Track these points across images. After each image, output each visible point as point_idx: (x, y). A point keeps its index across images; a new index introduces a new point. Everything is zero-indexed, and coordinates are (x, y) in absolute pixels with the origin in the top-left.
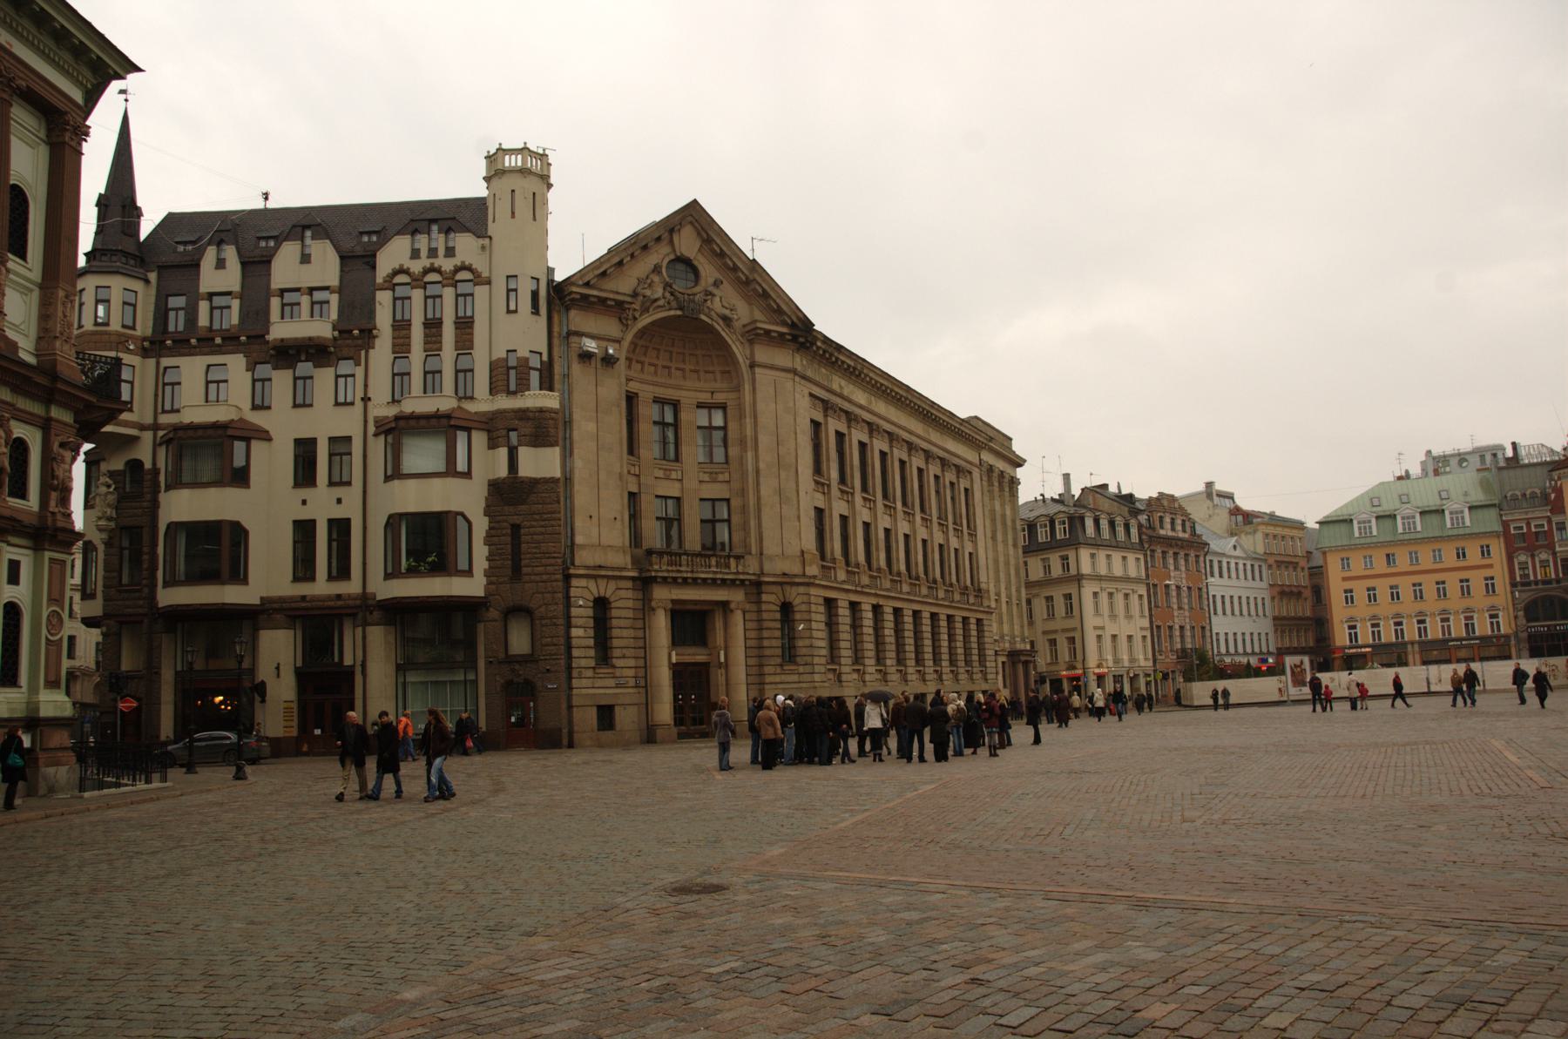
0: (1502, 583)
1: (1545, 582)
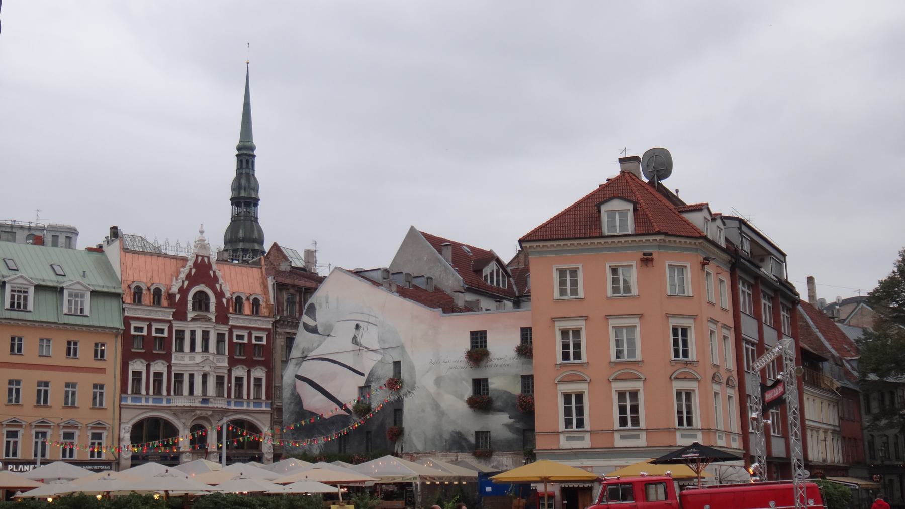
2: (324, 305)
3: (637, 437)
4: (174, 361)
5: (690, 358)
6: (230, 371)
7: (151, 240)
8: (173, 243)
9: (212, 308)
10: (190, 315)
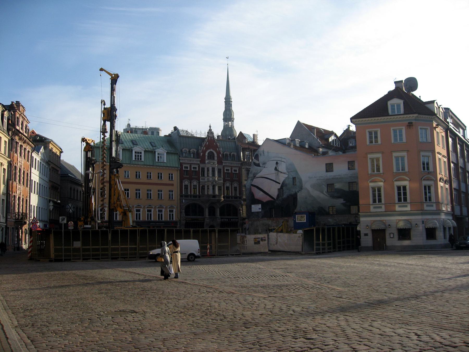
0: (176, 195)
1: (195, 196)
2: (262, 154)
3: (406, 206)
4: (201, 180)
5: (430, 171)
6: (224, 184)
7: (189, 131)
8: (199, 132)
9: (216, 158)
10: (207, 162)
